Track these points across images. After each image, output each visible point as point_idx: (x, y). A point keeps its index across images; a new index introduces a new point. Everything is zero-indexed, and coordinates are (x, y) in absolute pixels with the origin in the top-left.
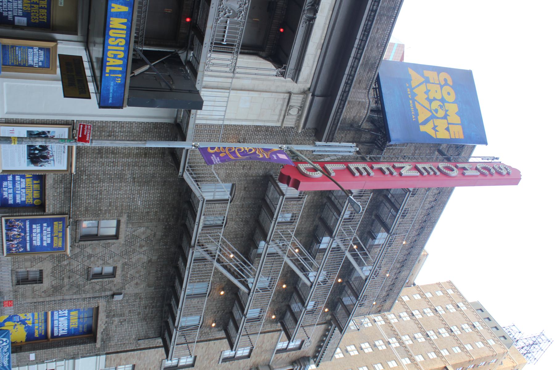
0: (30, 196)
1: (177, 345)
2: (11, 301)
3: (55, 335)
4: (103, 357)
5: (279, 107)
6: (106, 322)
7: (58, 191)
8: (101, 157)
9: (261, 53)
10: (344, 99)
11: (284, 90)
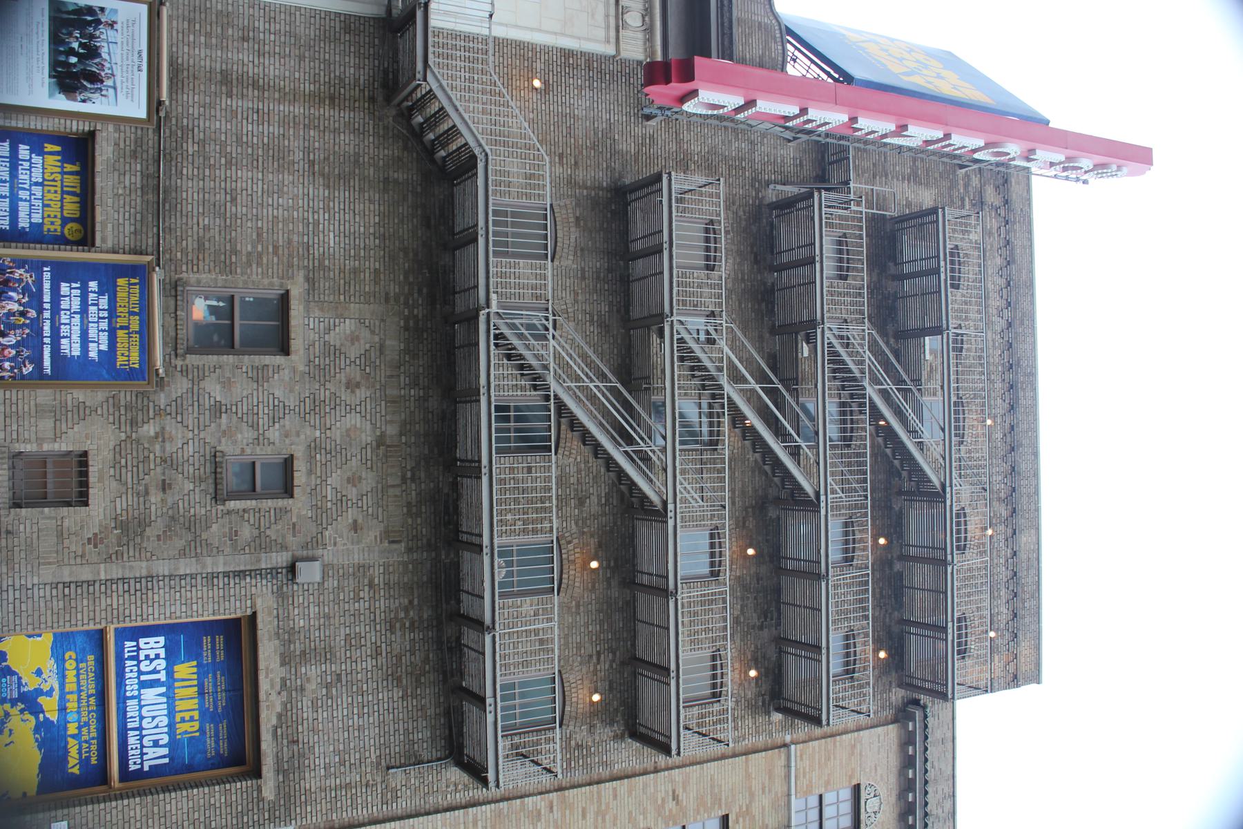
0: (55, 210)
3: (132, 768)
6: (284, 680)
7: (127, 183)
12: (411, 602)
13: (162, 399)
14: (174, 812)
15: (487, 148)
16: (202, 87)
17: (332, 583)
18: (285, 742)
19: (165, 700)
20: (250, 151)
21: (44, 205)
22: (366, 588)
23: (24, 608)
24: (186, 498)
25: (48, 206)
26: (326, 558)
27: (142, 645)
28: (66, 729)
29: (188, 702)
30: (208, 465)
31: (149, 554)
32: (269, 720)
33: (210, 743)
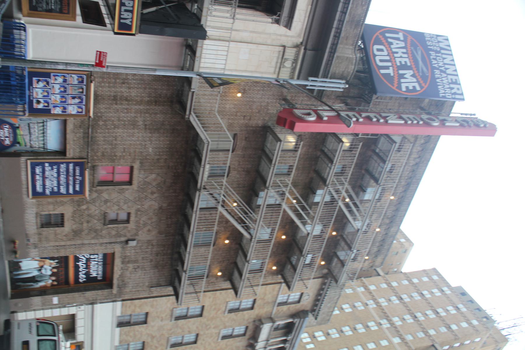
1: (186, 294)
4: (119, 304)
5: (275, 60)
6: (122, 269)
8: (116, 104)
9: (258, 7)
10: (333, 51)
11: (279, 43)
15: (209, 140)
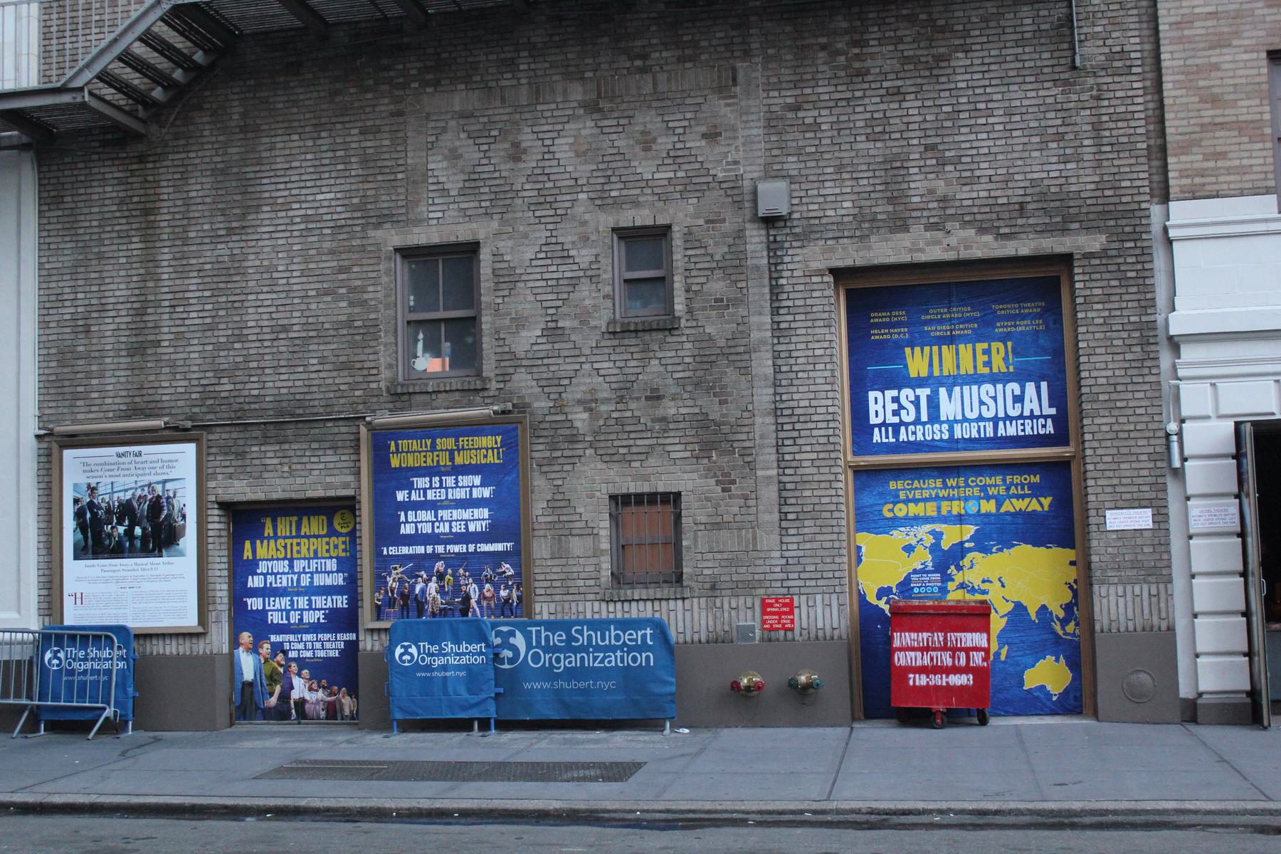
0: (320, 545)
2: (765, 605)
3: (1050, 429)
6: (930, 227)
7: (275, 461)
12: (823, 48)
13: (541, 405)
14: (1110, 373)
16: (152, 378)
17: (792, 164)
18: (1020, 222)
19: (957, 389)
20: (222, 313)
21: (316, 557)
22: (801, 114)
23: (813, 568)
24: (670, 368)
25: (316, 552)
26: (755, 175)
27: (880, 420)
28: (987, 515)
29: (965, 357)
30: (626, 342)
31: (746, 414)
32: (986, 245)
33: (1023, 326)
